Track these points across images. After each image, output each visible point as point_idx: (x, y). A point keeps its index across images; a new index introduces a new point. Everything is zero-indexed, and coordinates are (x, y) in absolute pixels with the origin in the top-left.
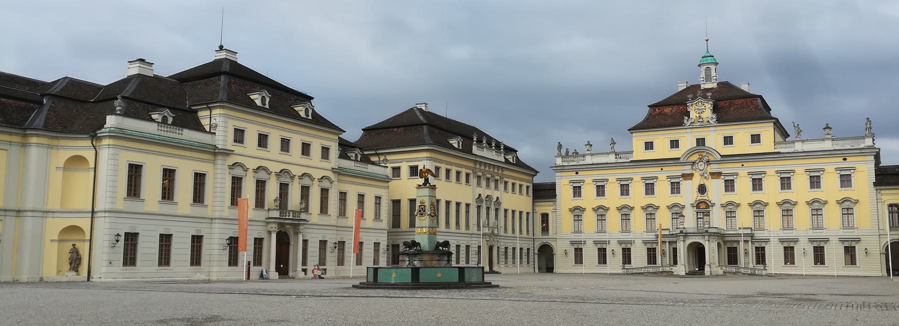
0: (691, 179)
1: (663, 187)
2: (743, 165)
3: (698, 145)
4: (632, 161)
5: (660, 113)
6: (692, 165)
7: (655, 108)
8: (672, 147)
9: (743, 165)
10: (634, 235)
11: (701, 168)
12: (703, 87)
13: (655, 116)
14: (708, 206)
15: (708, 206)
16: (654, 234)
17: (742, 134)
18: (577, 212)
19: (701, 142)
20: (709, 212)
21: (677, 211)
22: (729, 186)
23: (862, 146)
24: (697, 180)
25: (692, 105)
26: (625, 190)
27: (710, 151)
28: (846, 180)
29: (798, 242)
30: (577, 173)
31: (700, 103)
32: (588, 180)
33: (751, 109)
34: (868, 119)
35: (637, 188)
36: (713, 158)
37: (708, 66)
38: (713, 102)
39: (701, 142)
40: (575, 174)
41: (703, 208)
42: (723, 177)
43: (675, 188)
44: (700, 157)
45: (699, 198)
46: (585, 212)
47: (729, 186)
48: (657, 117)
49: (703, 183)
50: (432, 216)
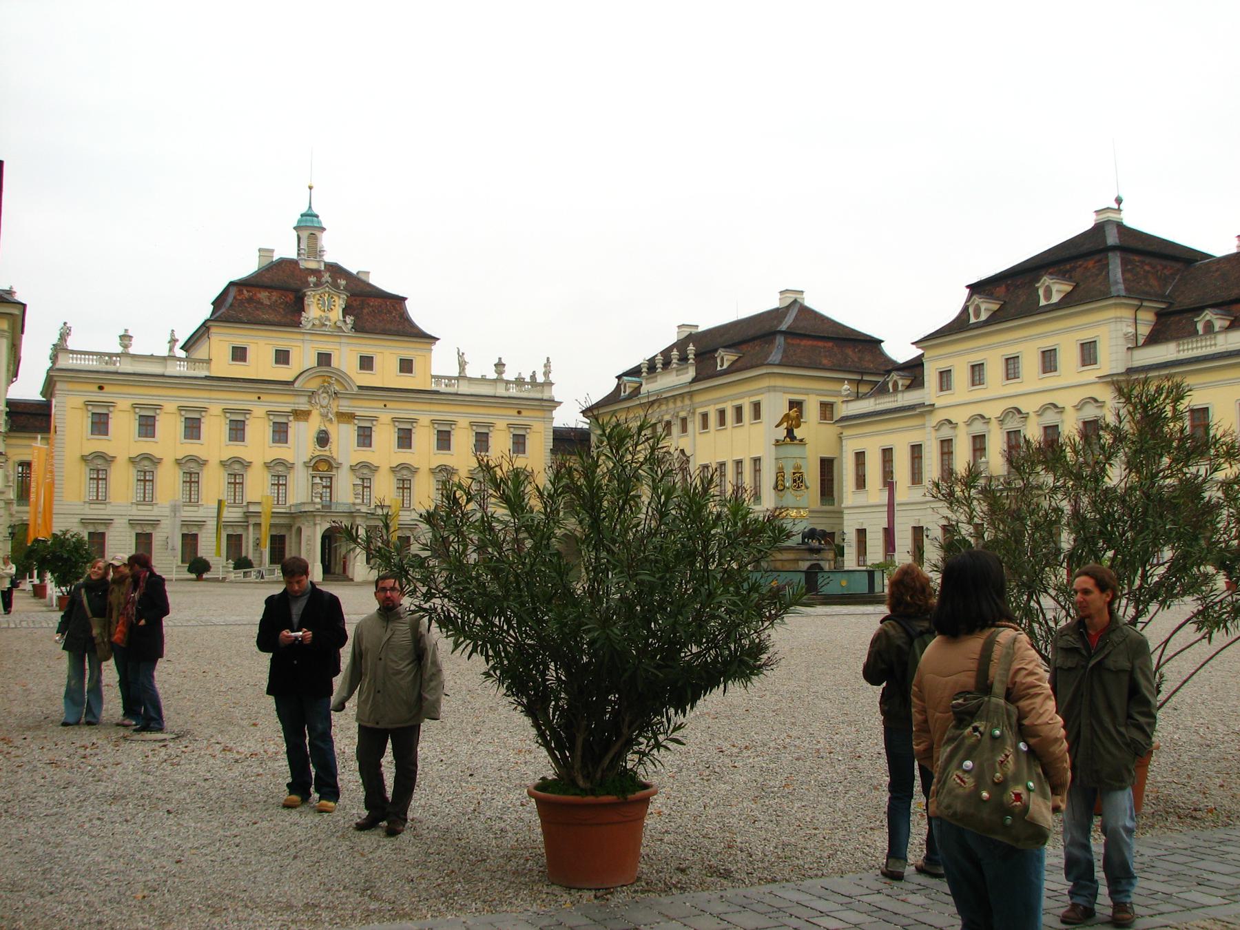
0: (306, 420)
1: (259, 431)
2: (385, 406)
3: (319, 364)
4: (207, 378)
5: (250, 300)
6: (309, 396)
7: (241, 288)
8: (277, 362)
9: (385, 406)
10: (205, 510)
11: (325, 402)
12: (304, 265)
13: (242, 302)
14: (331, 467)
15: (331, 467)
16: (240, 510)
17: (387, 355)
18: (98, 465)
19: (324, 359)
20: (331, 478)
21: (279, 471)
22: (365, 437)
23: (539, 396)
24: (314, 424)
25: (314, 296)
26: (193, 428)
27: (341, 377)
28: (519, 443)
29: (158, 526)
30: (101, 388)
31: (327, 295)
32: (124, 404)
33: (394, 317)
34: (548, 359)
35: (215, 429)
36: (341, 388)
37: (313, 232)
38: (347, 296)
39: (324, 359)
40: (97, 390)
41: (323, 467)
42: (356, 422)
43: (280, 433)
44: (326, 384)
45: (317, 453)
46: (159, 466)
47: (365, 437)
48: (246, 305)
49: (324, 428)
50: (781, 490)
